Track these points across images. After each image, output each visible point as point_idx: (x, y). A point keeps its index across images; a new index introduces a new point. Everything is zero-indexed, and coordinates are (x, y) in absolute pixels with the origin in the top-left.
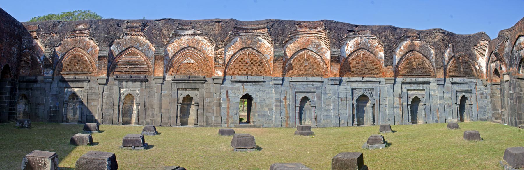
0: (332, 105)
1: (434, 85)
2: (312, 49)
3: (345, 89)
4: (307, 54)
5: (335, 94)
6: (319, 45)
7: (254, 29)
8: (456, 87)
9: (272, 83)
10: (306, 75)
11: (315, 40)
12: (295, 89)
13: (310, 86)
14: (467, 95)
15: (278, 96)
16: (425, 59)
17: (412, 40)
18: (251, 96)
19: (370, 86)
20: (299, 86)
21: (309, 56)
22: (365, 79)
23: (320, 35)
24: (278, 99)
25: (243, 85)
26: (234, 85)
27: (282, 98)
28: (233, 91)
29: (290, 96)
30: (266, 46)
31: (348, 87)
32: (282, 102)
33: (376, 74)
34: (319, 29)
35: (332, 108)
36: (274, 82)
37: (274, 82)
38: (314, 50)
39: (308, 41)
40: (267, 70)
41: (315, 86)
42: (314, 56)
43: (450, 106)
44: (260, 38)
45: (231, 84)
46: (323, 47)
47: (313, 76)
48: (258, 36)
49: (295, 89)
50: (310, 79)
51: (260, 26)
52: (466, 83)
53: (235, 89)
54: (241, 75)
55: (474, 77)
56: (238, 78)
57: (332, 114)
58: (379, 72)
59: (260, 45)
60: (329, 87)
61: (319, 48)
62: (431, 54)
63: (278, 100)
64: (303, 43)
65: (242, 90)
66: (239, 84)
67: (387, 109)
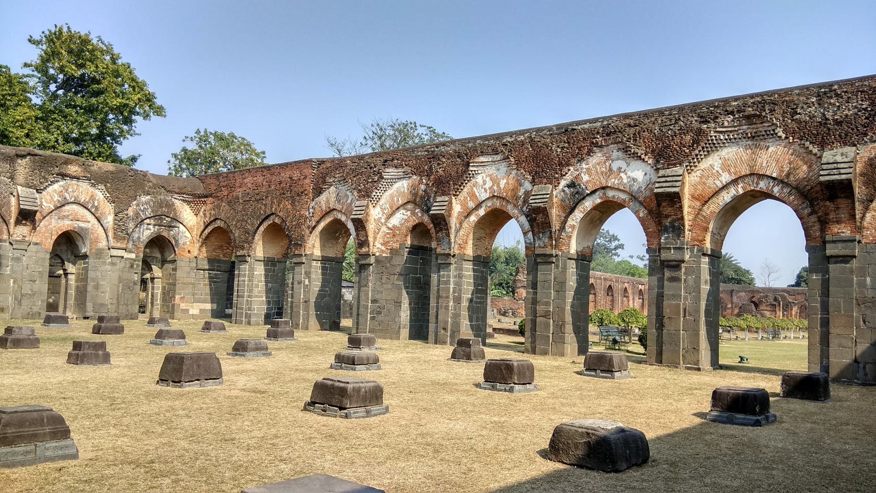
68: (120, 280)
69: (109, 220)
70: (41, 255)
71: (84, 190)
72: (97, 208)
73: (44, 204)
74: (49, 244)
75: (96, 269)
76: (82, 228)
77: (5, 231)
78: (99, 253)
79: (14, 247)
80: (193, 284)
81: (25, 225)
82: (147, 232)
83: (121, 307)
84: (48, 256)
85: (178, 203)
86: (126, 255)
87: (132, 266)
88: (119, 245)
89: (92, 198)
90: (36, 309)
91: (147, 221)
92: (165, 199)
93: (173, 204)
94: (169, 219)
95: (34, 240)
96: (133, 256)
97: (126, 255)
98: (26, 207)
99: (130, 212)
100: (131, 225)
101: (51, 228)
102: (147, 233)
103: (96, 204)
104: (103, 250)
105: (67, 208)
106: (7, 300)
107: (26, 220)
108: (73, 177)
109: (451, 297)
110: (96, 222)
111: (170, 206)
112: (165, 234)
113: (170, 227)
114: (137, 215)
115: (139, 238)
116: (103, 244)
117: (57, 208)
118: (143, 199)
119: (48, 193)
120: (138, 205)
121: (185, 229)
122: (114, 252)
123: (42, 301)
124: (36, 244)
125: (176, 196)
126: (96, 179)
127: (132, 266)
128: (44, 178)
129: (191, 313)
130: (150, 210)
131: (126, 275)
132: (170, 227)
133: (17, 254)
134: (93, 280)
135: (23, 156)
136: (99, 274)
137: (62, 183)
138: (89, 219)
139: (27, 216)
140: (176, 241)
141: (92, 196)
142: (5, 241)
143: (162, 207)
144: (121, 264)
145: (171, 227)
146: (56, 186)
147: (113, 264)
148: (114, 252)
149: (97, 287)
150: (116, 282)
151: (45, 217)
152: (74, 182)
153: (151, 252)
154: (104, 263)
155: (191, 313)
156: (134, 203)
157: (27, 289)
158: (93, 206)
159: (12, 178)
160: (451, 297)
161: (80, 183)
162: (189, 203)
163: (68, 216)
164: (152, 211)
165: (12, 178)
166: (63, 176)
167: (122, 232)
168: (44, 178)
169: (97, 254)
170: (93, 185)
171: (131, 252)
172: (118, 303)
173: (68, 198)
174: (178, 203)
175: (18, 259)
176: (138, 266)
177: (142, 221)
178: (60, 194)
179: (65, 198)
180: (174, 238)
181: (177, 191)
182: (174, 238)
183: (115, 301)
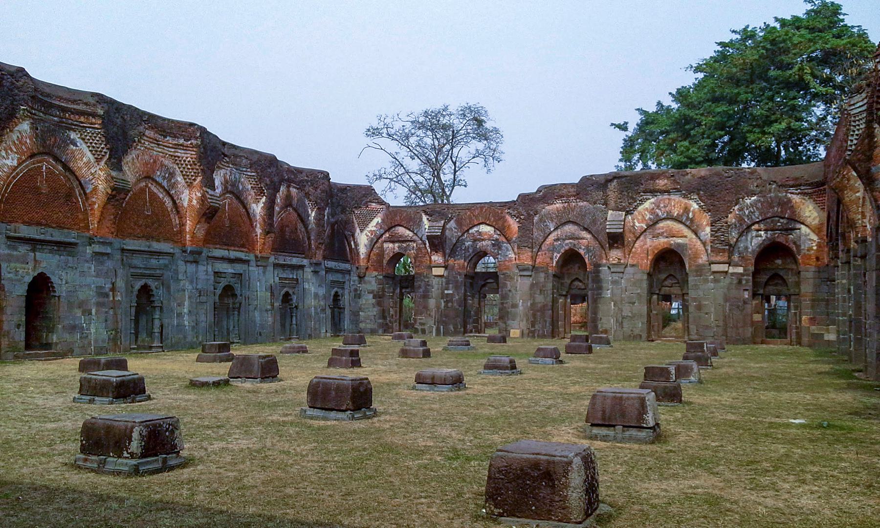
0: (186, 303)
1: (308, 270)
2: (160, 180)
3: (204, 272)
4: (149, 188)
5: (191, 282)
6: (172, 175)
7: (64, 110)
8: (331, 277)
9: (89, 250)
10: (148, 237)
11: (166, 162)
12: (131, 267)
13: (154, 262)
14: (340, 292)
15: (101, 281)
16: (300, 226)
17: (288, 187)
18: (49, 278)
19: (239, 268)
20: (137, 261)
21: (153, 195)
22: (233, 254)
23: (180, 153)
24: (101, 287)
25: (33, 250)
26: (15, 249)
27: (109, 286)
28: (13, 265)
29: (120, 283)
30: (86, 157)
31: (210, 269)
32: (107, 296)
33: (243, 246)
34: (182, 141)
35: (186, 310)
36: (97, 248)
37: (97, 248)
38: (165, 184)
39: (155, 162)
40: (81, 216)
41: (161, 262)
42: (161, 196)
43: (323, 310)
44: (73, 135)
45: (9, 247)
46: (179, 179)
47: (158, 241)
48: (70, 129)
49: (131, 267)
50: (156, 246)
51: (81, 107)
52: (337, 271)
53: (18, 260)
54: (29, 224)
55: (347, 261)
56: (26, 231)
57: (186, 323)
58: (247, 240)
59: (73, 153)
60: (182, 266)
61: (173, 181)
62: (309, 216)
63: (101, 293)
64: (146, 164)
65: (31, 266)
66: (23, 249)
67: (257, 314)
68: (726, 300)
69: (707, 232)
70: (638, 276)
71: (676, 203)
72: (692, 220)
73: (637, 224)
74: (646, 263)
75: (696, 287)
76: (679, 245)
77: (604, 256)
78: (700, 270)
79: (612, 270)
80: (827, 300)
81: (617, 248)
82: (756, 240)
83: (729, 330)
84: (645, 277)
85: (796, 199)
86: (732, 270)
87: (740, 282)
88: (719, 258)
89: (686, 210)
90: (637, 332)
91: (756, 226)
92: (776, 196)
93: (790, 201)
94: (785, 221)
95: (630, 261)
96: (740, 270)
97: (732, 270)
98: (612, 231)
99: (731, 219)
100: (734, 234)
101: (647, 246)
102: (756, 242)
103: (691, 215)
104: (704, 265)
105: (661, 225)
106: (609, 321)
107: (617, 243)
108: (663, 192)
109: (806, 302)
110: (694, 236)
111: (786, 204)
112: (781, 240)
113: (787, 230)
114: (740, 219)
115: (746, 248)
116: (703, 259)
117: (649, 227)
118: (748, 201)
119: (639, 213)
120: (741, 210)
121: (808, 230)
122: (715, 268)
123: (643, 323)
124: (633, 266)
125: (792, 190)
126: (687, 191)
127: (740, 282)
128: (632, 198)
129: (826, 338)
130: (757, 214)
131: (734, 293)
132: (787, 230)
133: (616, 277)
134: (695, 299)
135: (611, 181)
136: (701, 293)
137: (652, 200)
138: (685, 234)
139: (616, 240)
140: (798, 247)
141: (686, 208)
142: (604, 266)
143: (774, 207)
144: (725, 282)
145: (789, 230)
146: (647, 205)
147: (716, 281)
148: (715, 268)
149: (699, 308)
150: (721, 301)
151: (638, 238)
152: (666, 196)
153: (783, 263)
154: (706, 281)
155: (826, 338)
156: (736, 208)
157: (626, 312)
158: (688, 218)
159: (606, 204)
160: (806, 302)
161: (672, 197)
162: (810, 195)
163: (663, 233)
164: (761, 214)
165: (606, 204)
166: (654, 192)
167: (724, 247)
168: (632, 198)
169: (697, 271)
170: (685, 197)
171: (737, 265)
172: (726, 325)
173: (660, 214)
174: (796, 199)
175: (614, 282)
176: (747, 281)
177: (749, 228)
178: (652, 212)
179: (658, 215)
180: (795, 243)
181: (791, 183)
182: (795, 243)
183: (721, 323)
